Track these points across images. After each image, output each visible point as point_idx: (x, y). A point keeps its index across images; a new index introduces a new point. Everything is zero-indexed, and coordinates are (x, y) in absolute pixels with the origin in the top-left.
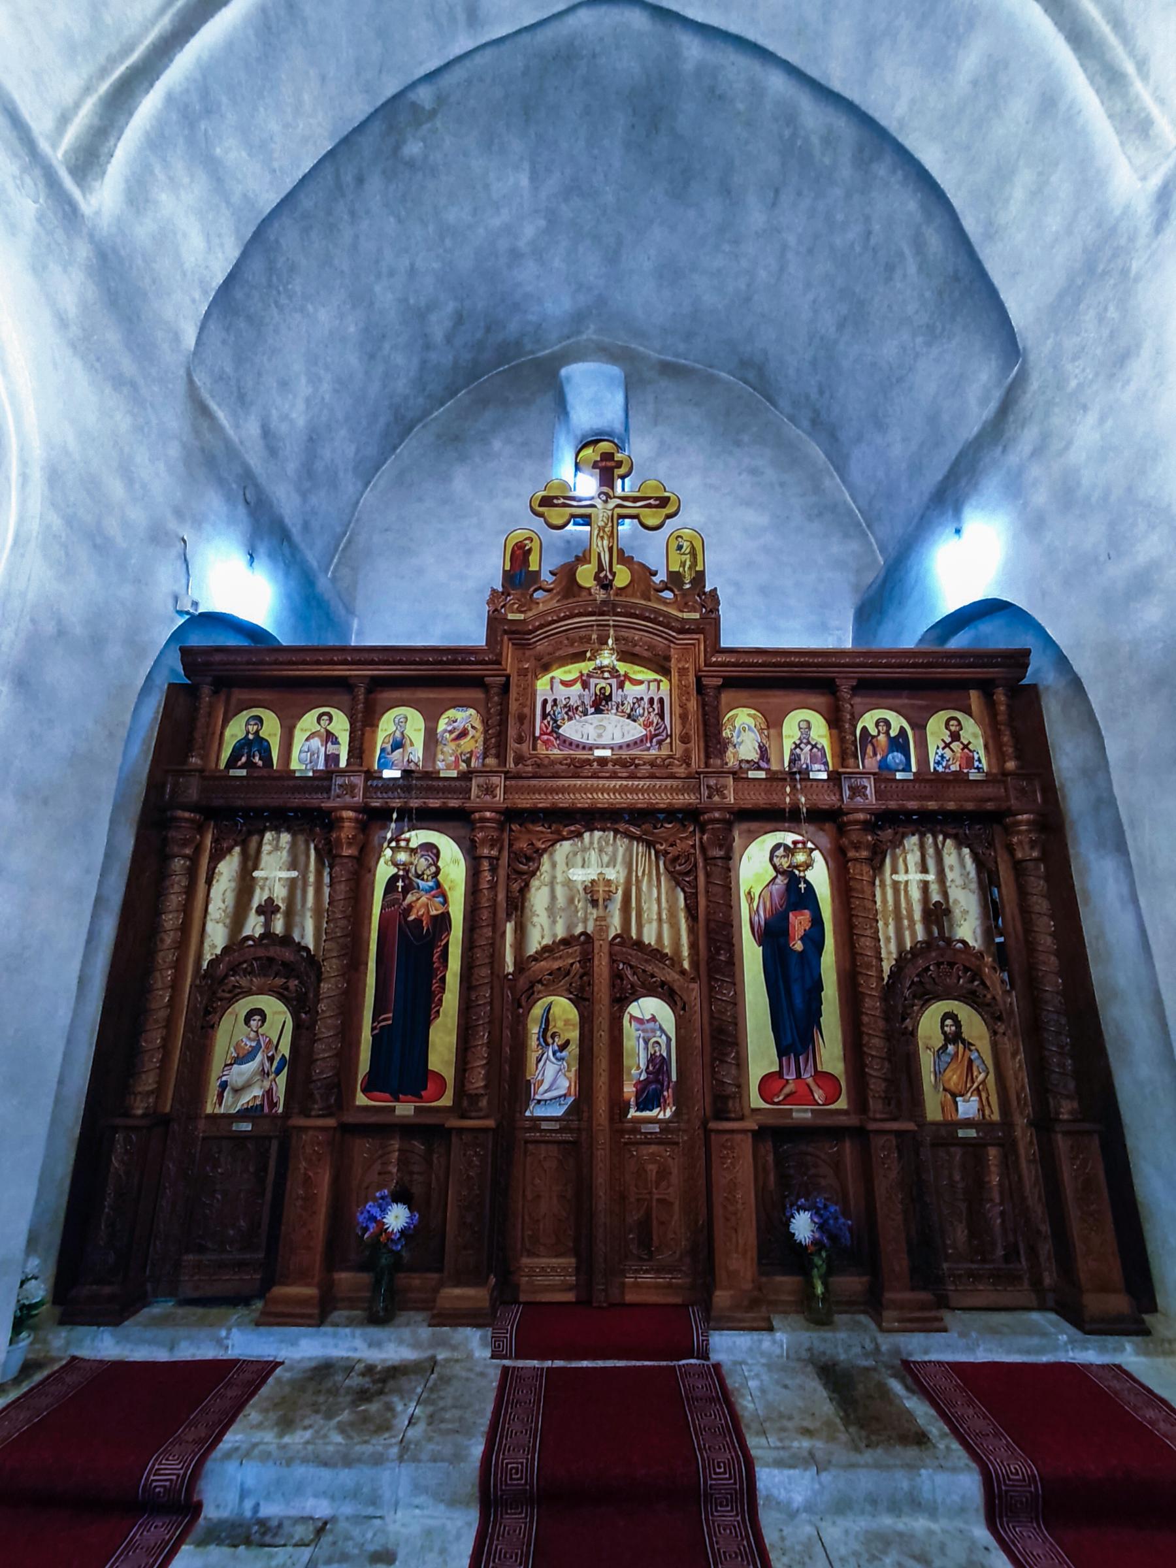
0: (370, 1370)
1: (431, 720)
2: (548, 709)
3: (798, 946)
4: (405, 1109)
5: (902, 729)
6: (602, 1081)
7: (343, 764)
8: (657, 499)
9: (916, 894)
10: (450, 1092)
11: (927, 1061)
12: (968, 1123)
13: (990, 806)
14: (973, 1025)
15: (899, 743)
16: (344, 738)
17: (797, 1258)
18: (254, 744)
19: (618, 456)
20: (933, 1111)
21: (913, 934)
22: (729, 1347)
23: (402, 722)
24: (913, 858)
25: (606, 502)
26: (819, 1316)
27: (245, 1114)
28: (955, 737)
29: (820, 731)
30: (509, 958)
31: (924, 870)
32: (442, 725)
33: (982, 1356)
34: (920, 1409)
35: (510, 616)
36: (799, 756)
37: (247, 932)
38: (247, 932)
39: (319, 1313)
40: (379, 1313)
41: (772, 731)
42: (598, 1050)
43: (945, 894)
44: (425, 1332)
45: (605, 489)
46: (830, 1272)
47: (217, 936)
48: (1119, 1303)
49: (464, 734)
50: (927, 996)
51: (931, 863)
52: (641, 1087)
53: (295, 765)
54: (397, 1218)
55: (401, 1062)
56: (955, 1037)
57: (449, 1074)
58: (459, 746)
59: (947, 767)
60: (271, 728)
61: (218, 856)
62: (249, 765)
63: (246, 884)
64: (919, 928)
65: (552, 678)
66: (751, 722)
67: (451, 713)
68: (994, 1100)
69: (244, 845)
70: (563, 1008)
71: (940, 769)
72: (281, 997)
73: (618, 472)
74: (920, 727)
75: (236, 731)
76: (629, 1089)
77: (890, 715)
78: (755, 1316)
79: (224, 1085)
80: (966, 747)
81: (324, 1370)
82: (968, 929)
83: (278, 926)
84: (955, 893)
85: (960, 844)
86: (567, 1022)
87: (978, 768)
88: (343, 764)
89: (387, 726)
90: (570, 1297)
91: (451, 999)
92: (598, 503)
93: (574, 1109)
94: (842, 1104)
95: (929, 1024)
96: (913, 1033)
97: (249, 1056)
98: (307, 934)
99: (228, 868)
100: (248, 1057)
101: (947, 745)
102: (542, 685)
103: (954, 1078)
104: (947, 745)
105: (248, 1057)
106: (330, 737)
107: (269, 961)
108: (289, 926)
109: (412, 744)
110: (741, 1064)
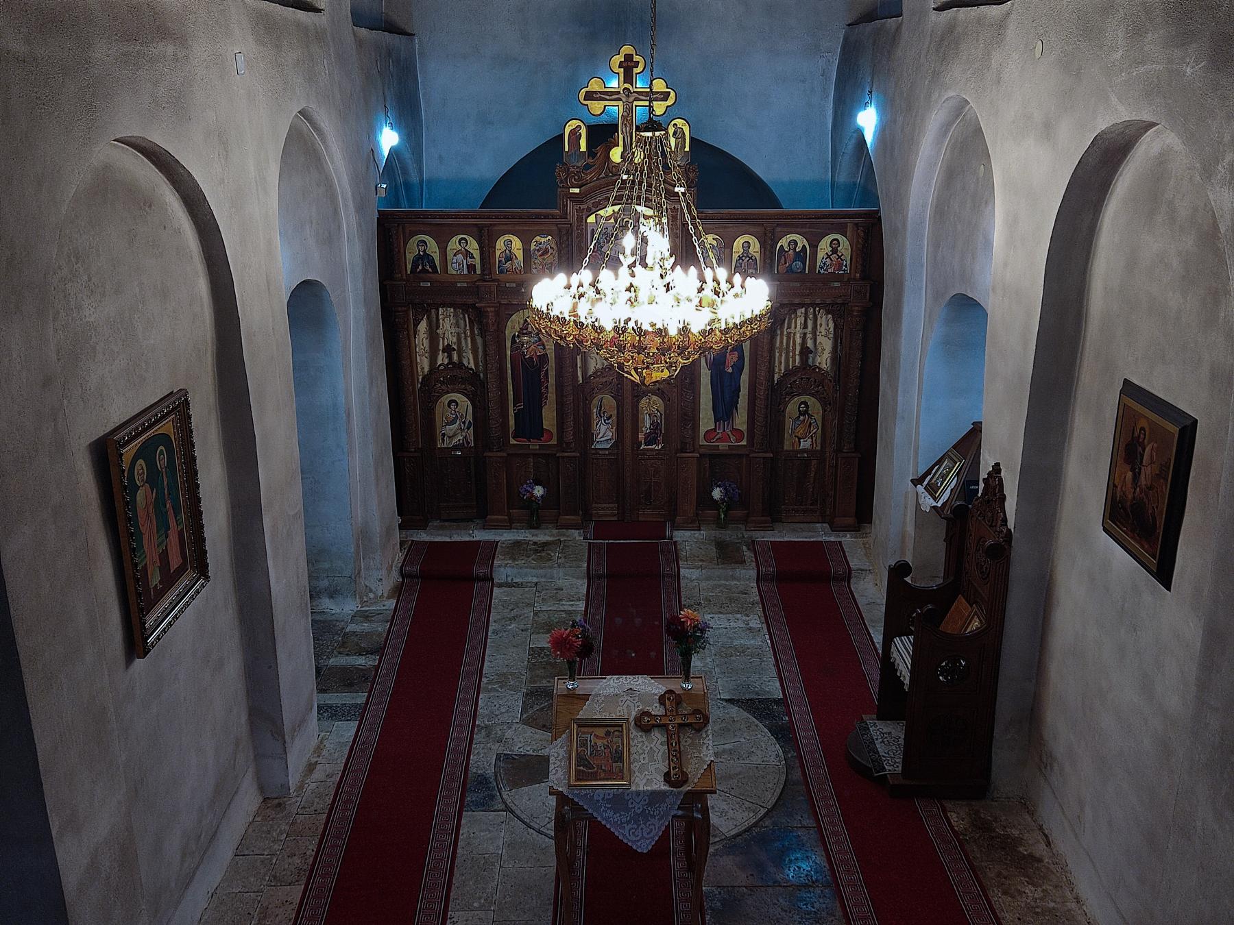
0: (535, 543)
1: (526, 244)
3: (730, 370)
4: (534, 445)
6: (628, 434)
7: (478, 272)
8: (662, 93)
9: (798, 340)
10: (555, 438)
11: (789, 423)
12: (804, 451)
13: (839, 301)
14: (815, 405)
15: (800, 256)
16: (476, 254)
17: (715, 504)
18: (425, 257)
19: (636, 58)
20: (787, 446)
21: (794, 361)
22: (679, 536)
23: (509, 244)
24: (800, 320)
25: (628, 96)
26: (721, 526)
27: (456, 448)
28: (834, 251)
29: (755, 247)
30: (580, 374)
31: (805, 326)
32: (533, 247)
33: (786, 539)
34: (748, 554)
35: (572, 190)
37: (440, 362)
38: (440, 362)
39: (509, 525)
40: (534, 525)
41: (727, 251)
42: (626, 420)
44: (555, 531)
45: (627, 85)
46: (729, 508)
47: (424, 364)
48: (850, 520)
49: (546, 252)
50: (792, 395)
51: (810, 323)
52: (647, 436)
53: (451, 271)
54: (539, 491)
55: (530, 424)
56: (806, 413)
57: (554, 431)
60: (433, 247)
61: (416, 326)
62: (424, 271)
63: (433, 337)
64: (797, 357)
66: (715, 243)
67: (538, 238)
68: (819, 441)
69: (428, 312)
70: (609, 400)
72: (463, 394)
73: (636, 70)
74: (814, 247)
75: (412, 250)
76: (641, 437)
77: (798, 238)
78: (694, 523)
79: (444, 435)
81: (517, 544)
82: (824, 360)
83: (455, 358)
84: (819, 339)
85: (828, 313)
86: (611, 407)
88: (478, 272)
89: (500, 244)
90: (615, 518)
91: (552, 396)
92: (622, 96)
93: (615, 445)
94: (744, 443)
95: (792, 408)
96: (784, 411)
97: (453, 422)
98: (469, 361)
99: (423, 326)
100: (454, 422)
101: (829, 257)
102: (592, 219)
103: (800, 431)
104: (829, 257)
105: (454, 422)
106: (468, 254)
107: (456, 376)
108: (460, 356)
110: (696, 427)
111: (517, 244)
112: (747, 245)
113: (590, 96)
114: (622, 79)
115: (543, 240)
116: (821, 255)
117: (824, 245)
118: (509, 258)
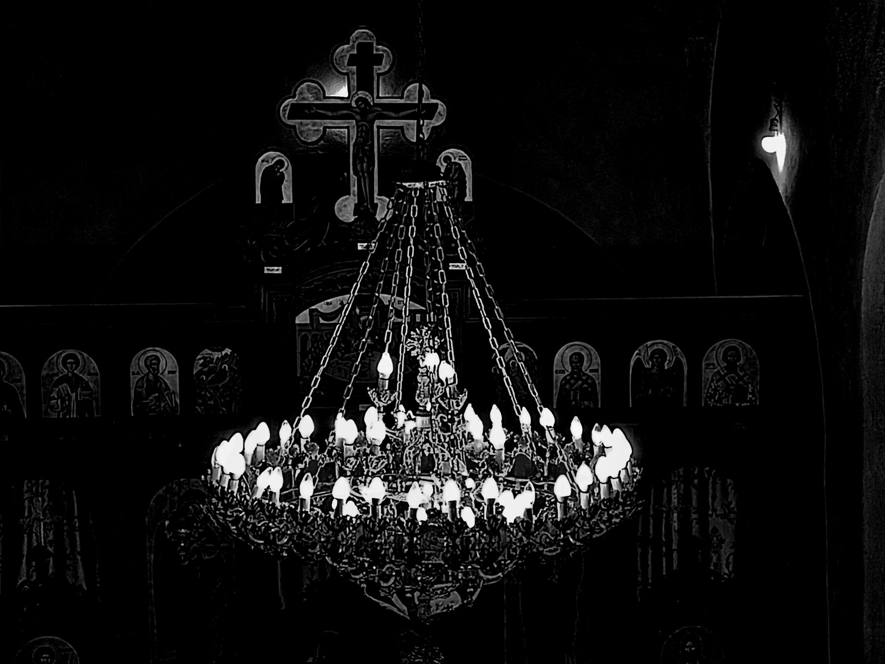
2: (309, 345)
5: (678, 360)
28: (731, 367)
29: (592, 363)
36: (568, 391)
43: (703, 521)
45: (361, 94)
58: (217, 388)
59: (720, 400)
65: (311, 311)
71: (711, 403)
80: (741, 378)
84: (715, 521)
87: (751, 401)
89: (138, 363)
101: (722, 378)
102: (302, 318)
109: (167, 388)
111: (168, 362)
112: (577, 360)
113: (298, 111)
114: (354, 83)
115: (217, 355)
116: (707, 374)
117: (714, 357)
118: (155, 384)
